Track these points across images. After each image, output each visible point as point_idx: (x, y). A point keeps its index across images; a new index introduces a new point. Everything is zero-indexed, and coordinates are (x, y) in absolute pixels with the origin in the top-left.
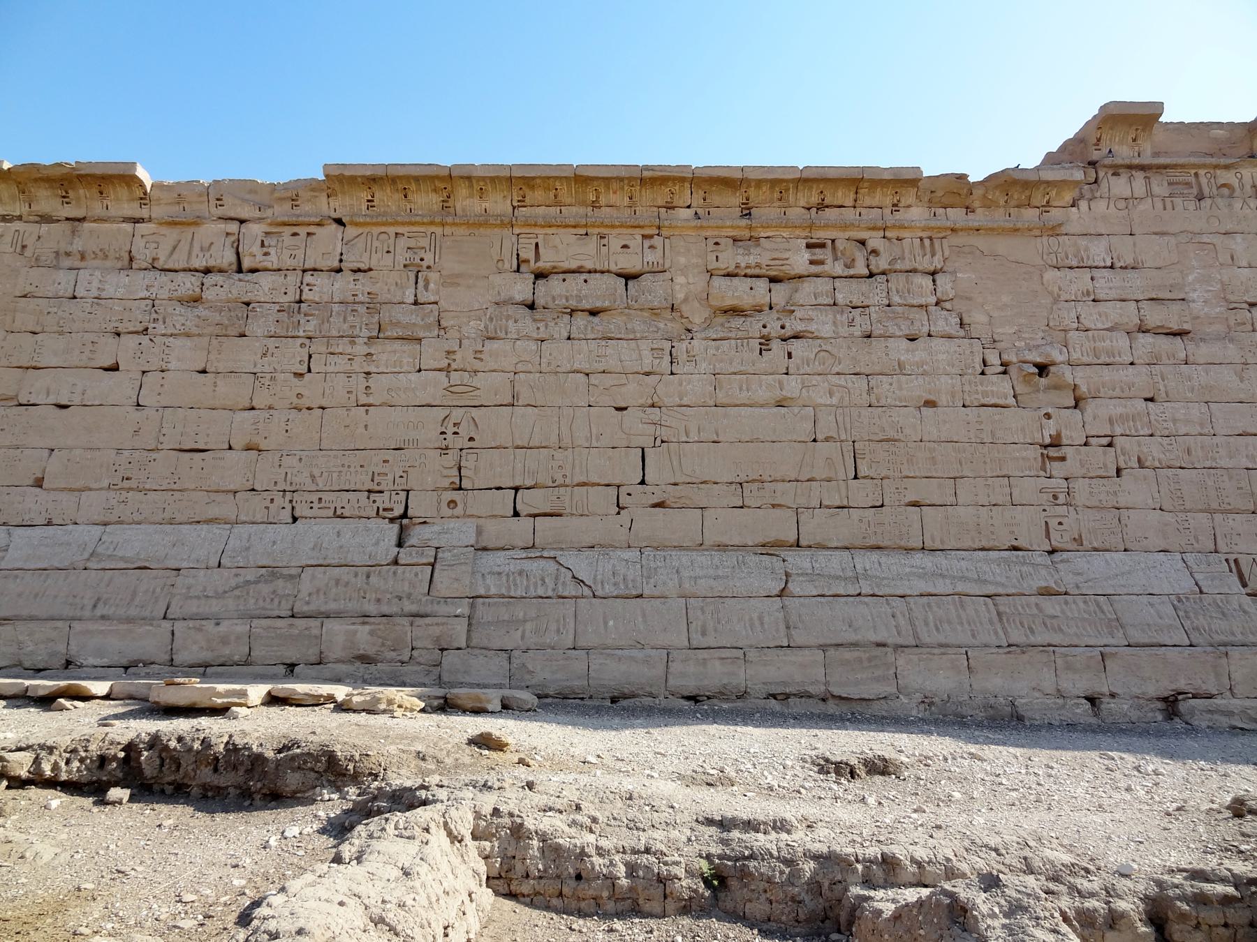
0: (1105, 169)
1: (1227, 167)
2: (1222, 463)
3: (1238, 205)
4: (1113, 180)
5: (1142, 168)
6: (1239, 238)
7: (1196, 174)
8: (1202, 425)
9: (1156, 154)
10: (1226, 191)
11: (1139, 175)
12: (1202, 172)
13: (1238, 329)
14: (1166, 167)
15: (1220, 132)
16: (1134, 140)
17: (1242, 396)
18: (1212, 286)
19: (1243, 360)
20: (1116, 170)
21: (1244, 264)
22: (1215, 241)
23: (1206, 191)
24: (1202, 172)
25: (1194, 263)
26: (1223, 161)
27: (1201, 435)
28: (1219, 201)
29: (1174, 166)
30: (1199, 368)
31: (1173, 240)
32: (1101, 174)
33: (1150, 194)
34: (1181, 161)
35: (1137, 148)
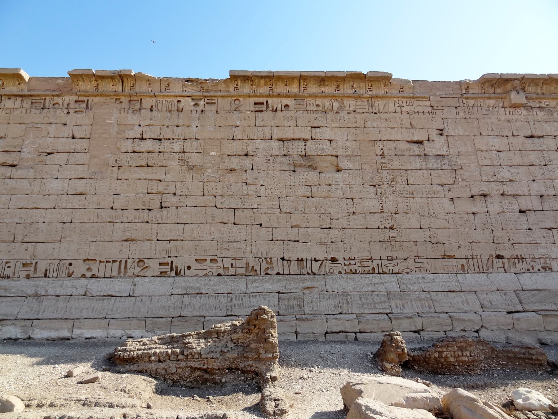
0: (5, 97)
1: (58, 96)
2: (6, 221)
3: (59, 111)
4: (7, 101)
5: (21, 96)
6: (54, 125)
7: (45, 99)
8: (4, 205)
9: (29, 90)
10: (56, 106)
11: (19, 99)
12: (47, 98)
13: (39, 163)
14: (31, 96)
15: (61, 82)
16: (19, 84)
17: (28, 192)
18: (35, 146)
19: (35, 177)
20: (9, 97)
21: (52, 136)
22: (42, 127)
23: (47, 105)
24: (47, 98)
25: (31, 136)
26: (54, 93)
27: (3, 209)
28: (51, 110)
29: (35, 96)
30: (14, 180)
31: (24, 126)
32: (3, 98)
33: (22, 107)
34: (35, 93)
35: (21, 88)
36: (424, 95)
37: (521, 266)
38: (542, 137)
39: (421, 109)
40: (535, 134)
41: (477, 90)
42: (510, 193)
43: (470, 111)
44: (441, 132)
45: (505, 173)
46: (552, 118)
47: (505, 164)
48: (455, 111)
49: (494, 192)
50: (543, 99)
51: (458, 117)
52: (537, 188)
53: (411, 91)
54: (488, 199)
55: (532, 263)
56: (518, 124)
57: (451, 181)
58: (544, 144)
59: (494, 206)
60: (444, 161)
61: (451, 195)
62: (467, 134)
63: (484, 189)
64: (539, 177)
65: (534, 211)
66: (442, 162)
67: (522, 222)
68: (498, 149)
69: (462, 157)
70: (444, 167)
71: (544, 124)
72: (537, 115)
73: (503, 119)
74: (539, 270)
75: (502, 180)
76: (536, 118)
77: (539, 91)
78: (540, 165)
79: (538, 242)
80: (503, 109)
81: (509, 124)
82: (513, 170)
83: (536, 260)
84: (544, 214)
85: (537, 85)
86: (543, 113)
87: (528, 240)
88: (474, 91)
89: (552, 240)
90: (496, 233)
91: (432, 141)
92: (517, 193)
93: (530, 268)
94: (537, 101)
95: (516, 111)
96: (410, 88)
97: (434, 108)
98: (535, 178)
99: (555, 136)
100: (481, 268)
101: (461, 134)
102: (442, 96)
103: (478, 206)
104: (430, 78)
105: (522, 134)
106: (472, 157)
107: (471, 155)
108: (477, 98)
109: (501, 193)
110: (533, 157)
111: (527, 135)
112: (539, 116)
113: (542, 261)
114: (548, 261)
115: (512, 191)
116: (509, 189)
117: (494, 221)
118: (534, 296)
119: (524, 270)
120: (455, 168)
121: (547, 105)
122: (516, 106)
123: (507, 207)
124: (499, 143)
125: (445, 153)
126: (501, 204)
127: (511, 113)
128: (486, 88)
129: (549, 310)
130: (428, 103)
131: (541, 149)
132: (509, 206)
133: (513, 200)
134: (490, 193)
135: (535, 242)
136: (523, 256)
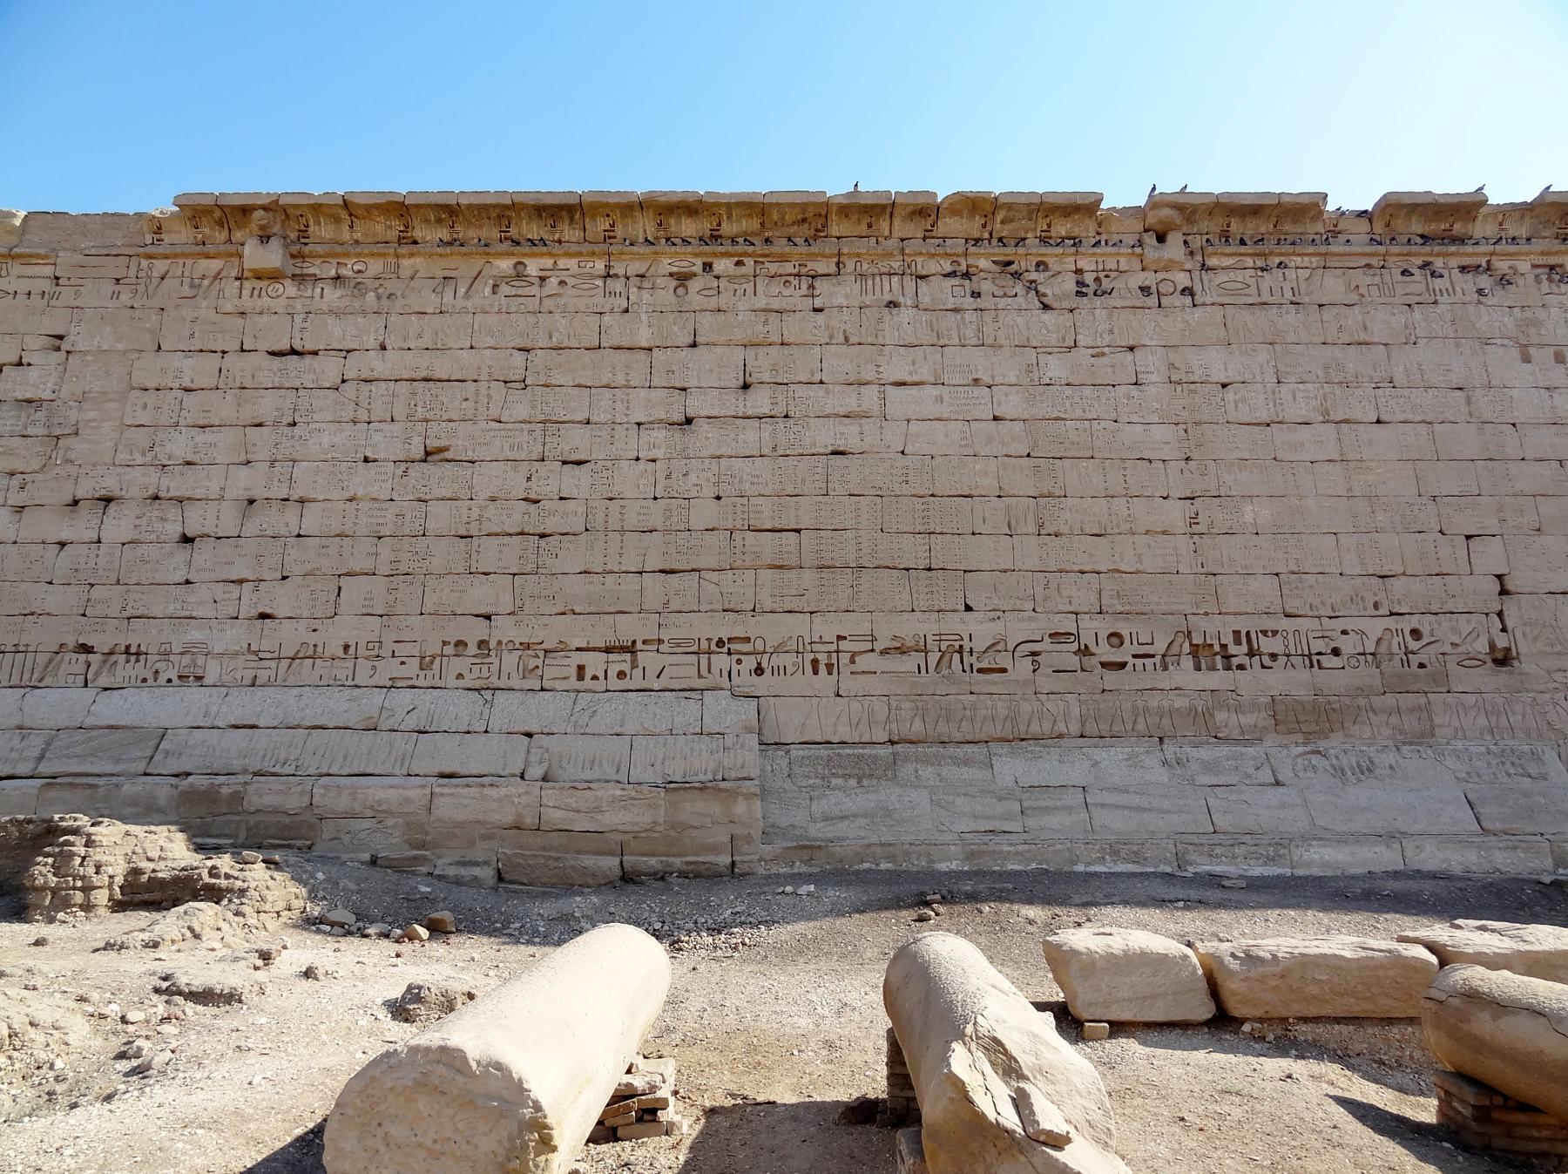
36: (33, 251)
37: (126, 670)
38: (315, 353)
39: (23, 285)
40: (298, 347)
41: (182, 235)
42: (172, 493)
43: (150, 290)
44: (57, 342)
45: (179, 445)
46: (357, 305)
47: (190, 421)
48: (109, 287)
49: (134, 492)
50: (347, 255)
51: (113, 304)
52: (244, 482)
53: (14, 240)
54: (112, 505)
55: (158, 666)
56: (264, 320)
57: (36, 464)
58: (312, 370)
59: (118, 525)
60: (39, 414)
61: (16, 499)
62: (120, 347)
63: (110, 485)
64: (263, 453)
65: (219, 538)
66: (32, 418)
67: (177, 564)
68: (187, 384)
69: (84, 405)
70: (29, 431)
71: (329, 322)
72: (322, 297)
73: (228, 308)
74: (170, 681)
75: (165, 462)
76: (318, 304)
77: (346, 235)
78: (276, 423)
79: (195, 614)
80: (237, 283)
81: (240, 321)
82: (202, 437)
83: (172, 657)
84: (236, 547)
85: (337, 220)
86: (339, 293)
87: (171, 609)
88: (175, 238)
89: (232, 611)
90: (97, 593)
91: (29, 365)
92: (188, 494)
93: (150, 676)
94: (334, 261)
95: (271, 288)
96: (10, 233)
97: (60, 281)
98: (250, 457)
99: (348, 352)
100: (26, 676)
101: (105, 348)
102: (87, 252)
103: (80, 527)
104: (75, 207)
105: (263, 346)
106: (114, 405)
107: (111, 400)
108: (176, 256)
109: (151, 492)
110: (266, 406)
111: (275, 348)
112: (325, 299)
113: (186, 659)
114: (200, 660)
115: (178, 489)
116: (172, 485)
117: (102, 562)
118: (90, 739)
119: (133, 681)
120: (58, 432)
121: (360, 271)
122: (274, 276)
123: (150, 528)
124: (193, 370)
125: (47, 395)
126: (138, 522)
127: (256, 293)
128: (207, 231)
129: (88, 775)
130: (48, 271)
131: (297, 384)
132: (158, 525)
133: (173, 512)
134: (123, 493)
135: (187, 614)
136: (143, 649)
